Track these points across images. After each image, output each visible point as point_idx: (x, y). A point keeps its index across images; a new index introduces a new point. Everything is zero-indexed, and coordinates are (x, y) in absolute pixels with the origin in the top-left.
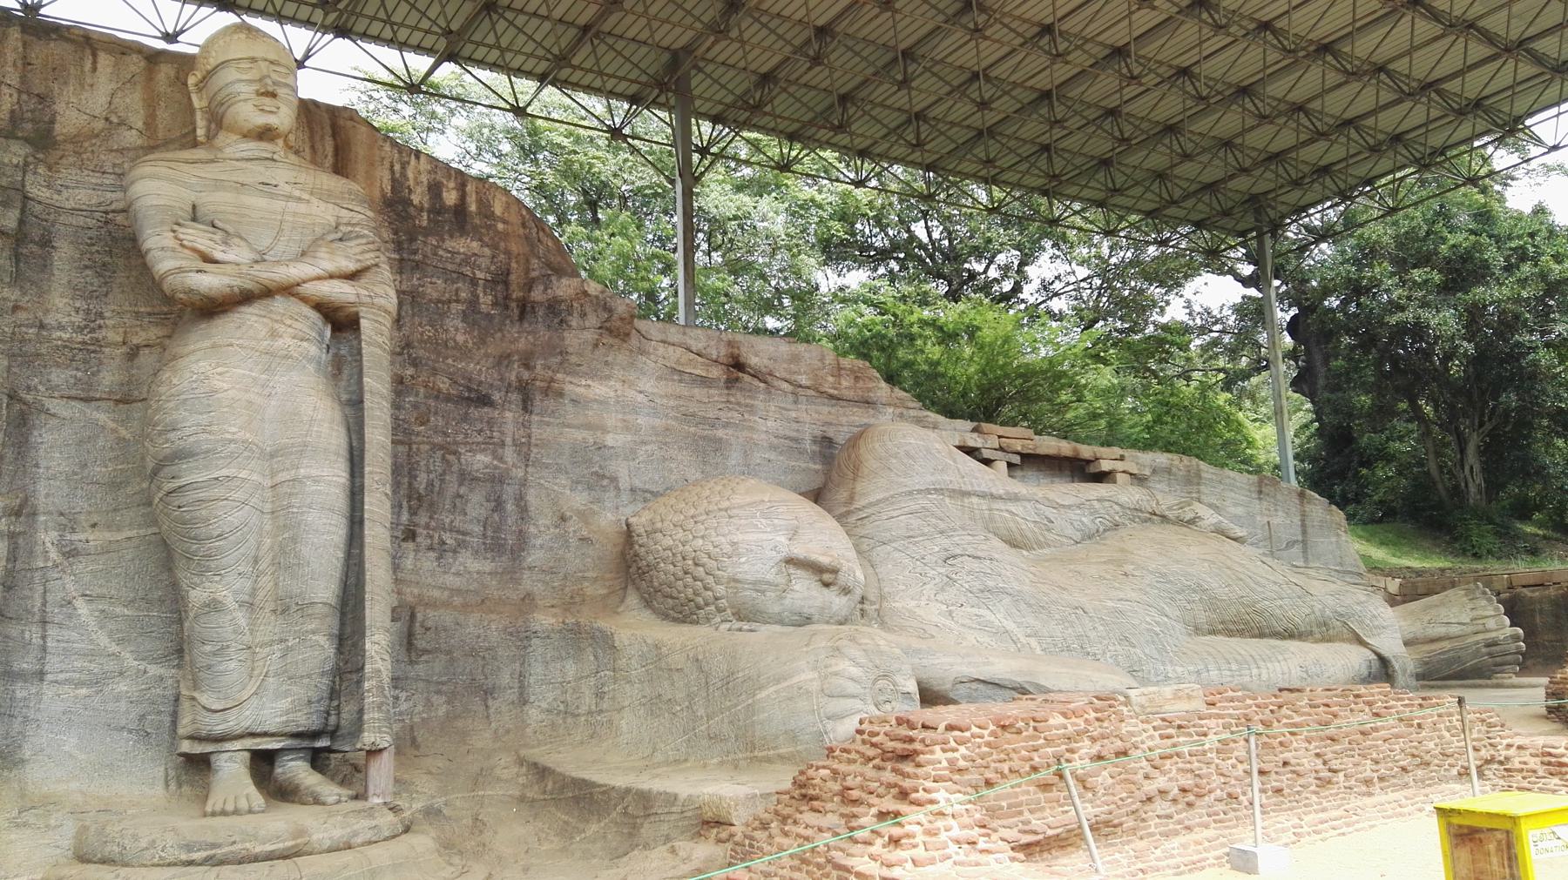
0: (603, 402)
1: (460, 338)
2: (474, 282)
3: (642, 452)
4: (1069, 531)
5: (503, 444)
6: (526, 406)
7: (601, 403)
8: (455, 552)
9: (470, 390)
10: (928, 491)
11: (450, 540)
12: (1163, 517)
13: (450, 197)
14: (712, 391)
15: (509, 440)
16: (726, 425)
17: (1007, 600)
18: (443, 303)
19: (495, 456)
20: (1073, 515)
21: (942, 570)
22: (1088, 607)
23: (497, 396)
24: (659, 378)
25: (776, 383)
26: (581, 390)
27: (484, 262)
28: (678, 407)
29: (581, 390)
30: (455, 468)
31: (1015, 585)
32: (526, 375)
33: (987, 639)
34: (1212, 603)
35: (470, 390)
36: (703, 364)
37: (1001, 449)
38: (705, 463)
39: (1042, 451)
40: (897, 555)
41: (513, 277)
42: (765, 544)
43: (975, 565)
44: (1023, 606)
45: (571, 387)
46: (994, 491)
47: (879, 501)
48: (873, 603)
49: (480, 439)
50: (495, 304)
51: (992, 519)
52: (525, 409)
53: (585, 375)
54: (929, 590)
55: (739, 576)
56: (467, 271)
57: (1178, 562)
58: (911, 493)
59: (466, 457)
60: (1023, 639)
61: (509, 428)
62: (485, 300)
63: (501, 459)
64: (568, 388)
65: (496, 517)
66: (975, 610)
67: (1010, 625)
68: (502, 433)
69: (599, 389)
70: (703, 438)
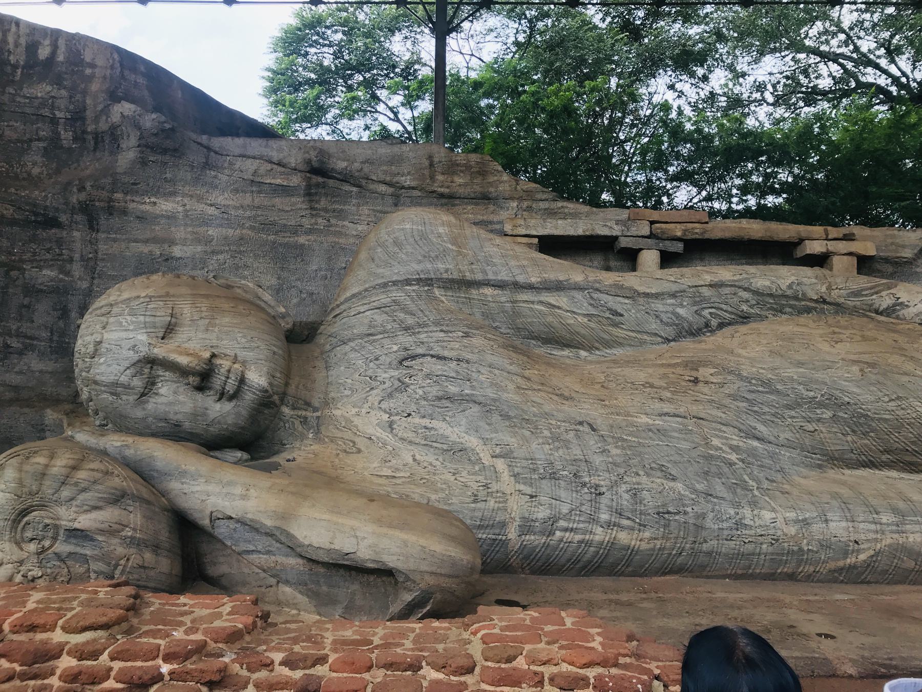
0: (171, 217)
1: (36, 171)
2: (54, 121)
3: (213, 263)
4: (654, 326)
5: (71, 260)
6: (92, 225)
7: (168, 217)
8: (21, 353)
9: (36, 214)
10: (408, 282)
11: (15, 343)
12: (837, 305)
13: (44, 53)
14: (293, 199)
15: (77, 256)
16: (310, 232)
17: (476, 409)
18: (22, 142)
19: (62, 271)
20: (658, 306)
21: (396, 373)
22: (599, 422)
23: (63, 218)
24: (236, 191)
25: (372, 186)
26: (148, 207)
27: (62, 103)
28: (255, 217)
29: (148, 207)
30: (20, 282)
31: (491, 393)
32: (83, 196)
33: (431, 458)
34: (860, 422)
35: (36, 214)
36: (281, 173)
37: (652, 236)
38: (282, 269)
39: (717, 235)
40: (352, 355)
41: (88, 113)
42: (123, 344)
43: (438, 367)
44: (496, 418)
45: (132, 206)
46: (521, 279)
47: (354, 296)
48: (316, 410)
49: (49, 256)
50: (75, 139)
51: (516, 314)
52: (91, 228)
53: (145, 193)
54: (375, 397)
55: (98, 378)
56: (46, 112)
57: (800, 364)
58: (385, 285)
59: (31, 272)
60: (487, 460)
61: (78, 246)
62: (66, 136)
63: (68, 273)
64: (132, 206)
65: (61, 324)
66: (426, 422)
67: (472, 441)
68: (71, 250)
69: (166, 206)
70: (285, 245)
